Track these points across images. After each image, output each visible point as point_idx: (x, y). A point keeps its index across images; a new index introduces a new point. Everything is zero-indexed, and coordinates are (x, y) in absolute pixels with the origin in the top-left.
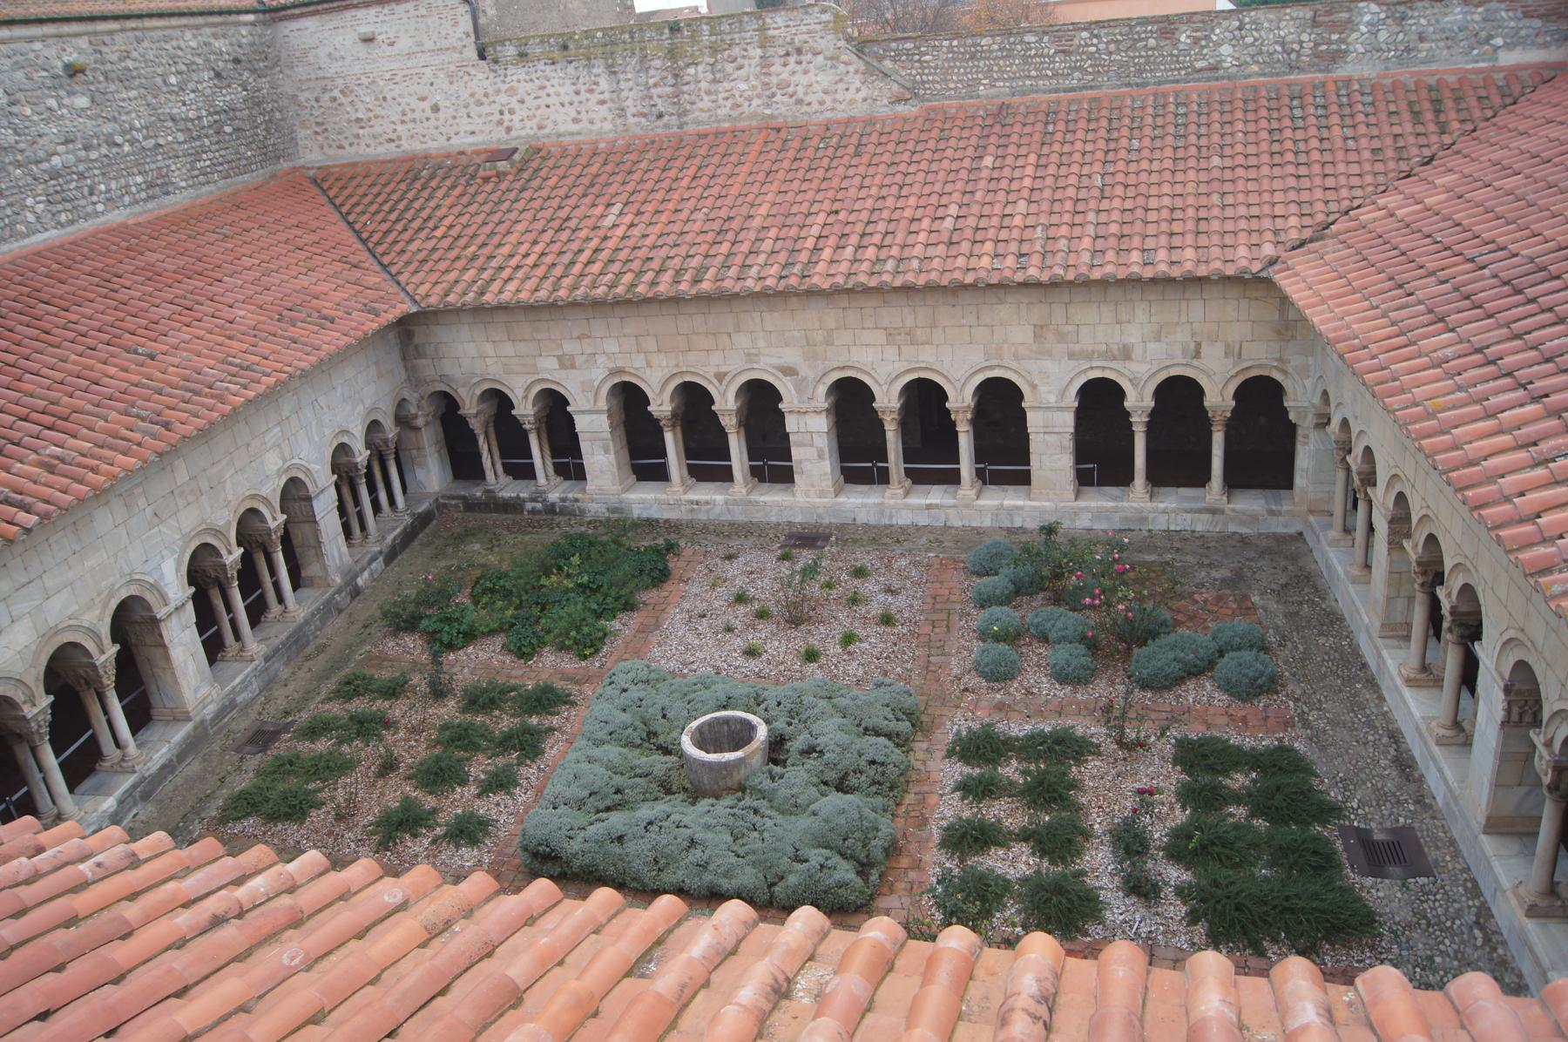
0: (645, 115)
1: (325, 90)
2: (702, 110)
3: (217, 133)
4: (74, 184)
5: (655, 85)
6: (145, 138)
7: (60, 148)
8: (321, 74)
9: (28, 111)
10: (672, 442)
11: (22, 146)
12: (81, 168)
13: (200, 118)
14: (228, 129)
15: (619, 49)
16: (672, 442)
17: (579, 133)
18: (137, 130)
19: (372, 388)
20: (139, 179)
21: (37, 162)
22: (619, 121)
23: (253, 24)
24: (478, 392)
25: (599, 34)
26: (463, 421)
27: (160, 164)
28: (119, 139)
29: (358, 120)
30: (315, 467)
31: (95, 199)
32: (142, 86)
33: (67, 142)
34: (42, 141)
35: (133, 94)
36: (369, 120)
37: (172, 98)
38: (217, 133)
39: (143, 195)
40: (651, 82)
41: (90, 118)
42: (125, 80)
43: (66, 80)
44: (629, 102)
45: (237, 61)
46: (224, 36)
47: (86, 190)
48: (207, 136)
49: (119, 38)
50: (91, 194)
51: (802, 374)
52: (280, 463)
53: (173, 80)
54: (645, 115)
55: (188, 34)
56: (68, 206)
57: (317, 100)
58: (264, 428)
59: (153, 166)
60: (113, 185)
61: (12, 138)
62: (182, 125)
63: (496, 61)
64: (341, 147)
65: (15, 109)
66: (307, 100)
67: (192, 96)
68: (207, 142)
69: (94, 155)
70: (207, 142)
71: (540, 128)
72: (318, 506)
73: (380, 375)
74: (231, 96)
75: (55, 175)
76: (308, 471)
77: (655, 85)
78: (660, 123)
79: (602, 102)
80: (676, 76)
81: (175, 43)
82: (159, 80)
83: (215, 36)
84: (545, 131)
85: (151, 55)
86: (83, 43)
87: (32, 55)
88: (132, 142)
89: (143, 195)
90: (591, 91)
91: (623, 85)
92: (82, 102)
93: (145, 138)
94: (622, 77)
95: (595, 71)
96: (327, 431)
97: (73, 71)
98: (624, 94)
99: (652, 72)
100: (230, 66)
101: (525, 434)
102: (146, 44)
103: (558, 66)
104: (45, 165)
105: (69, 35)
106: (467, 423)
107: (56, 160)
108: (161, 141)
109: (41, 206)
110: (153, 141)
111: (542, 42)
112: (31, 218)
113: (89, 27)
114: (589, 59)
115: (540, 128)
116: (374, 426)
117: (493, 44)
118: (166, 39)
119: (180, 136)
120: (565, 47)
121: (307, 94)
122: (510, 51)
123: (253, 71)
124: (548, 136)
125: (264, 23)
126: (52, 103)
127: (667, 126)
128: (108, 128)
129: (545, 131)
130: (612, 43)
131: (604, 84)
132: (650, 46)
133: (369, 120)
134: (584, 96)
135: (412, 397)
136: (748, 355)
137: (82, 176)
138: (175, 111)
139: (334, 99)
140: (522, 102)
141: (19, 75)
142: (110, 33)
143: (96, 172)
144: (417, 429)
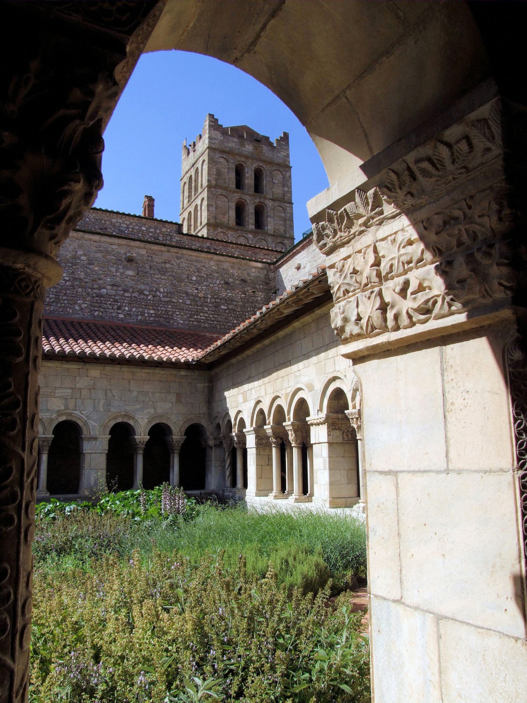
3: (216, 307)
4: (110, 302)
6: (163, 297)
7: (108, 287)
9: (97, 269)
11: (87, 280)
12: (117, 298)
13: (205, 298)
18: (160, 292)
19: (168, 405)
20: (152, 312)
21: (92, 289)
27: (168, 309)
28: (147, 293)
30: (91, 423)
31: (119, 311)
32: (171, 276)
33: (113, 285)
34: (100, 282)
35: (162, 277)
37: (191, 285)
39: (152, 319)
41: (133, 280)
42: (163, 271)
43: (126, 263)
45: (244, 281)
46: (239, 269)
47: (115, 307)
48: (207, 306)
49: (167, 254)
50: (119, 308)
52: (63, 408)
53: (194, 278)
56: (102, 310)
58: (58, 385)
59: (163, 309)
60: (134, 310)
61: (82, 277)
62: (192, 297)
65: (91, 267)
67: (205, 287)
69: (126, 294)
70: (206, 309)
72: (87, 447)
73: (179, 400)
75: (100, 296)
76: (86, 423)
81: (202, 264)
82: (184, 276)
83: (232, 267)
85: (184, 265)
86: (143, 252)
87: (110, 249)
88: (154, 296)
89: (152, 319)
92: (130, 273)
93: (163, 297)
96: (113, 410)
97: (130, 260)
100: (237, 282)
102: (182, 260)
104: (95, 291)
105: (134, 246)
107: (104, 291)
108: (174, 300)
109: (86, 305)
110: (169, 299)
112: (77, 308)
113: (148, 246)
118: (196, 261)
119: (188, 302)
126: (113, 270)
128: (143, 287)
137: (116, 301)
141: (99, 255)
142: (161, 251)
143: (125, 301)
144: (211, 448)
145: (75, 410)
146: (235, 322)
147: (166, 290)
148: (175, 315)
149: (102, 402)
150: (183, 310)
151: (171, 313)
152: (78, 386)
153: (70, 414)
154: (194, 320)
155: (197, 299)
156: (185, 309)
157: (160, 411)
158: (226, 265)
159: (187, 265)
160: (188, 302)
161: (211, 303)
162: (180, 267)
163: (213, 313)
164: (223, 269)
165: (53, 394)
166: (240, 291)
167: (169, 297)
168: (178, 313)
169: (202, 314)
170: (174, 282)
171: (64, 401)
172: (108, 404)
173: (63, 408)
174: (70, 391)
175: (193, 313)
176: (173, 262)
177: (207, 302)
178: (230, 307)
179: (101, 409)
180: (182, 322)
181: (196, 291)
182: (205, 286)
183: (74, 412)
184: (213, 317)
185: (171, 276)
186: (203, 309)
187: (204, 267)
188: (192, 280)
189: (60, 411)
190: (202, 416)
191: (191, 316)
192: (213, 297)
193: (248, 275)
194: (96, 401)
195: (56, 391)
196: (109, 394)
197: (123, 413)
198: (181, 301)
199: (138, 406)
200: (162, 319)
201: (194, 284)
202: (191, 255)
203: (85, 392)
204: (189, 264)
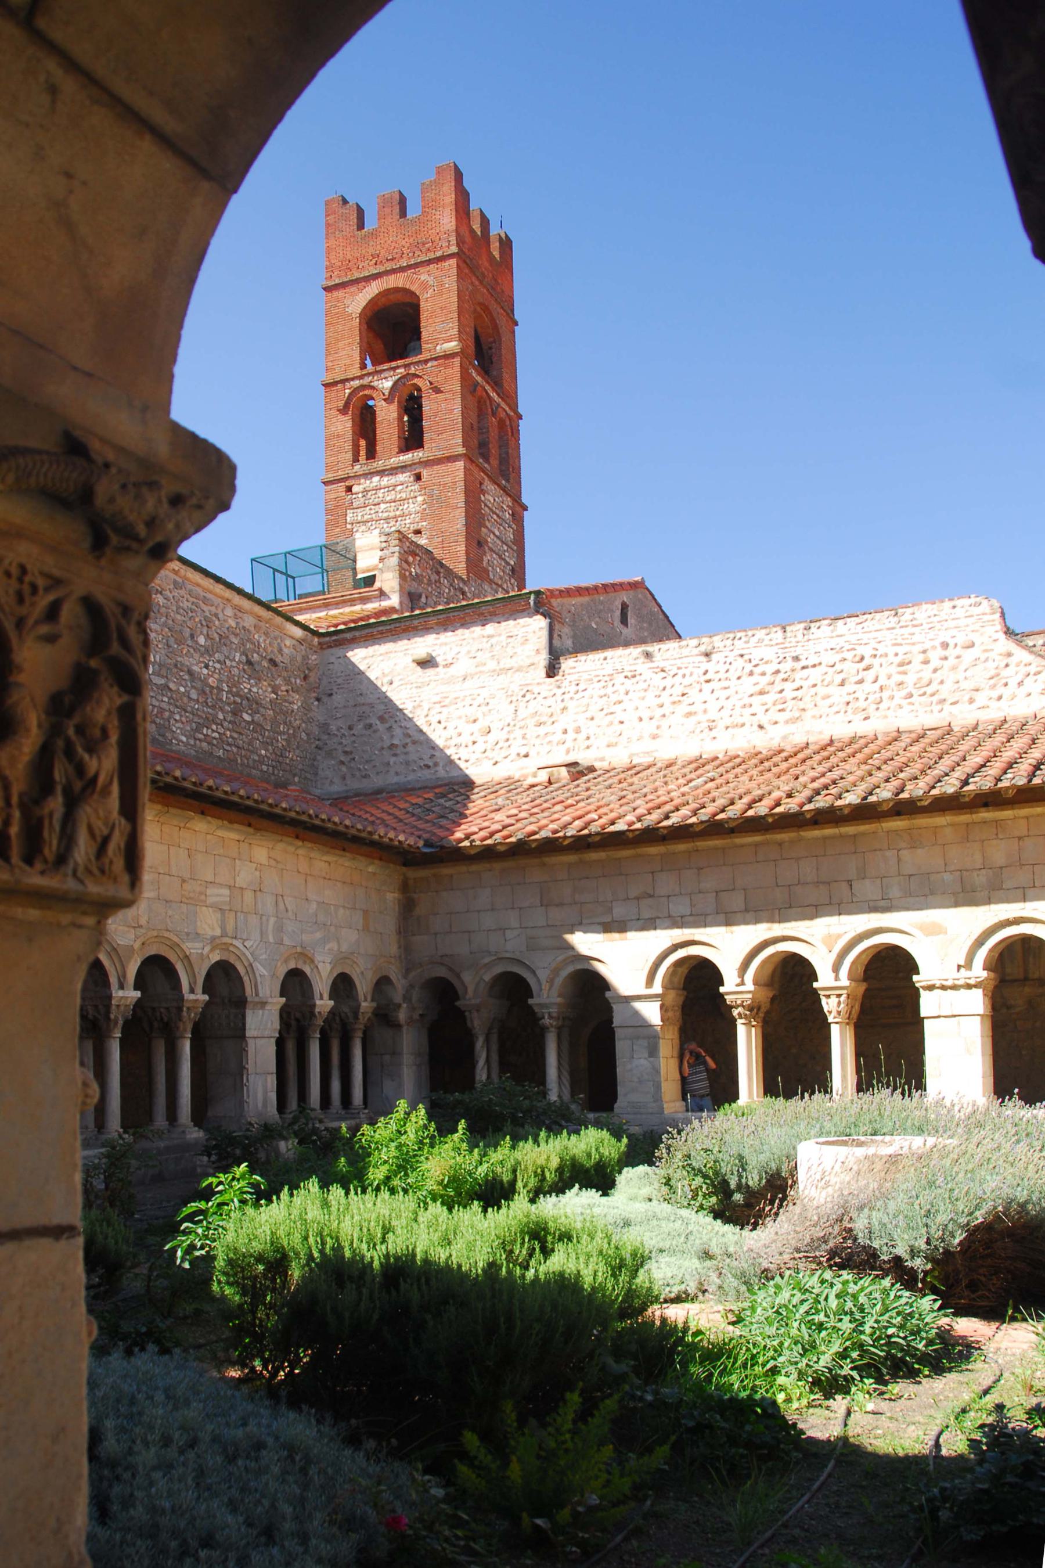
1: (360, 718)
3: (235, 713)
8: (361, 700)
10: (747, 1045)
14: (247, 717)
16: (747, 1045)
23: (300, 642)
24: (487, 977)
26: (460, 1016)
27: (164, 705)
29: (392, 746)
36: (405, 746)
37: (196, 656)
38: (235, 713)
45: (273, 662)
46: (266, 634)
48: (222, 709)
52: (218, 932)
53: (202, 640)
55: (229, 612)
57: (350, 728)
62: (199, 685)
64: (366, 776)
66: (339, 729)
67: (218, 666)
68: (221, 716)
73: (366, 928)
74: (262, 691)
82: (187, 633)
85: (186, 605)
96: (287, 941)
100: (265, 664)
101: (541, 1033)
102: (182, 592)
106: (464, 1018)
108: (172, 686)
110: (163, 681)
116: (343, 985)
119: (194, 695)
121: (340, 723)
123: (287, 681)
125: (311, 646)
133: (405, 746)
135: (400, 983)
138: (195, 668)
139: (370, 726)
145: (236, 938)
146: (263, 752)
147: (158, 659)
148: (172, 721)
149: (272, 920)
150: (186, 711)
151: (167, 714)
152: (240, 881)
153: (225, 948)
154: (201, 736)
155: (207, 690)
156: (189, 709)
157: (344, 948)
158: (249, 622)
159: (189, 604)
160: (194, 695)
161: (229, 704)
162: (178, 607)
163: (231, 726)
164: (244, 627)
165: (203, 897)
166: (269, 685)
167: (163, 677)
168: (177, 717)
169: (214, 727)
170: (172, 641)
171: (219, 915)
172: (280, 929)
173: (218, 932)
174: (227, 892)
175: (201, 721)
176: (168, 593)
177: (221, 700)
178: (257, 717)
179: (271, 940)
180: (184, 739)
181: (205, 671)
182: (219, 662)
183: (235, 942)
184: (231, 737)
185: (165, 624)
186: (216, 716)
187: (216, 615)
188: (197, 643)
189: (214, 938)
190: (393, 960)
191: (198, 730)
192: (229, 692)
193: (280, 651)
194: (264, 918)
195: (209, 892)
196: (281, 906)
197: (299, 950)
198: (182, 689)
199: (318, 935)
200: (154, 726)
201: (202, 655)
202: (198, 585)
203: (249, 896)
204: (193, 603)
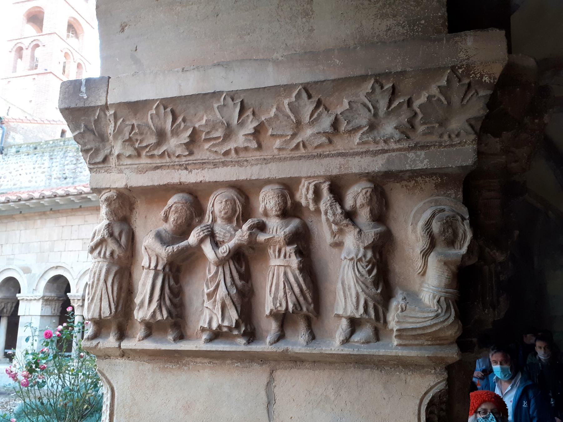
0: (59, 178)
2: (84, 176)
5: (67, 164)
15: (57, 149)
17: (29, 187)
22: (48, 181)
25: (51, 142)
40: (66, 163)
44: (54, 173)
51: (33, 272)
54: (59, 178)
63: (6, 155)
71: (14, 185)
77: (67, 164)
78: (65, 181)
79: (43, 172)
80: (77, 160)
84: (15, 187)
90: (40, 167)
91: (54, 164)
94: (54, 160)
95: (44, 158)
98: (53, 169)
99: (67, 158)
103: (30, 156)
111: (27, 146)
114: (43, 153)
115: (14, 185)
117: (7, 147)
120: (36, 148)
122: (14, 150)
124: (16, 189)
127: (67, 183)
129: (15, 187)
130: (56, 146)
131: (47, 163)
132: (70, 147)
134: (37, 169)
136: (9, 259)
140: (10, 173)
